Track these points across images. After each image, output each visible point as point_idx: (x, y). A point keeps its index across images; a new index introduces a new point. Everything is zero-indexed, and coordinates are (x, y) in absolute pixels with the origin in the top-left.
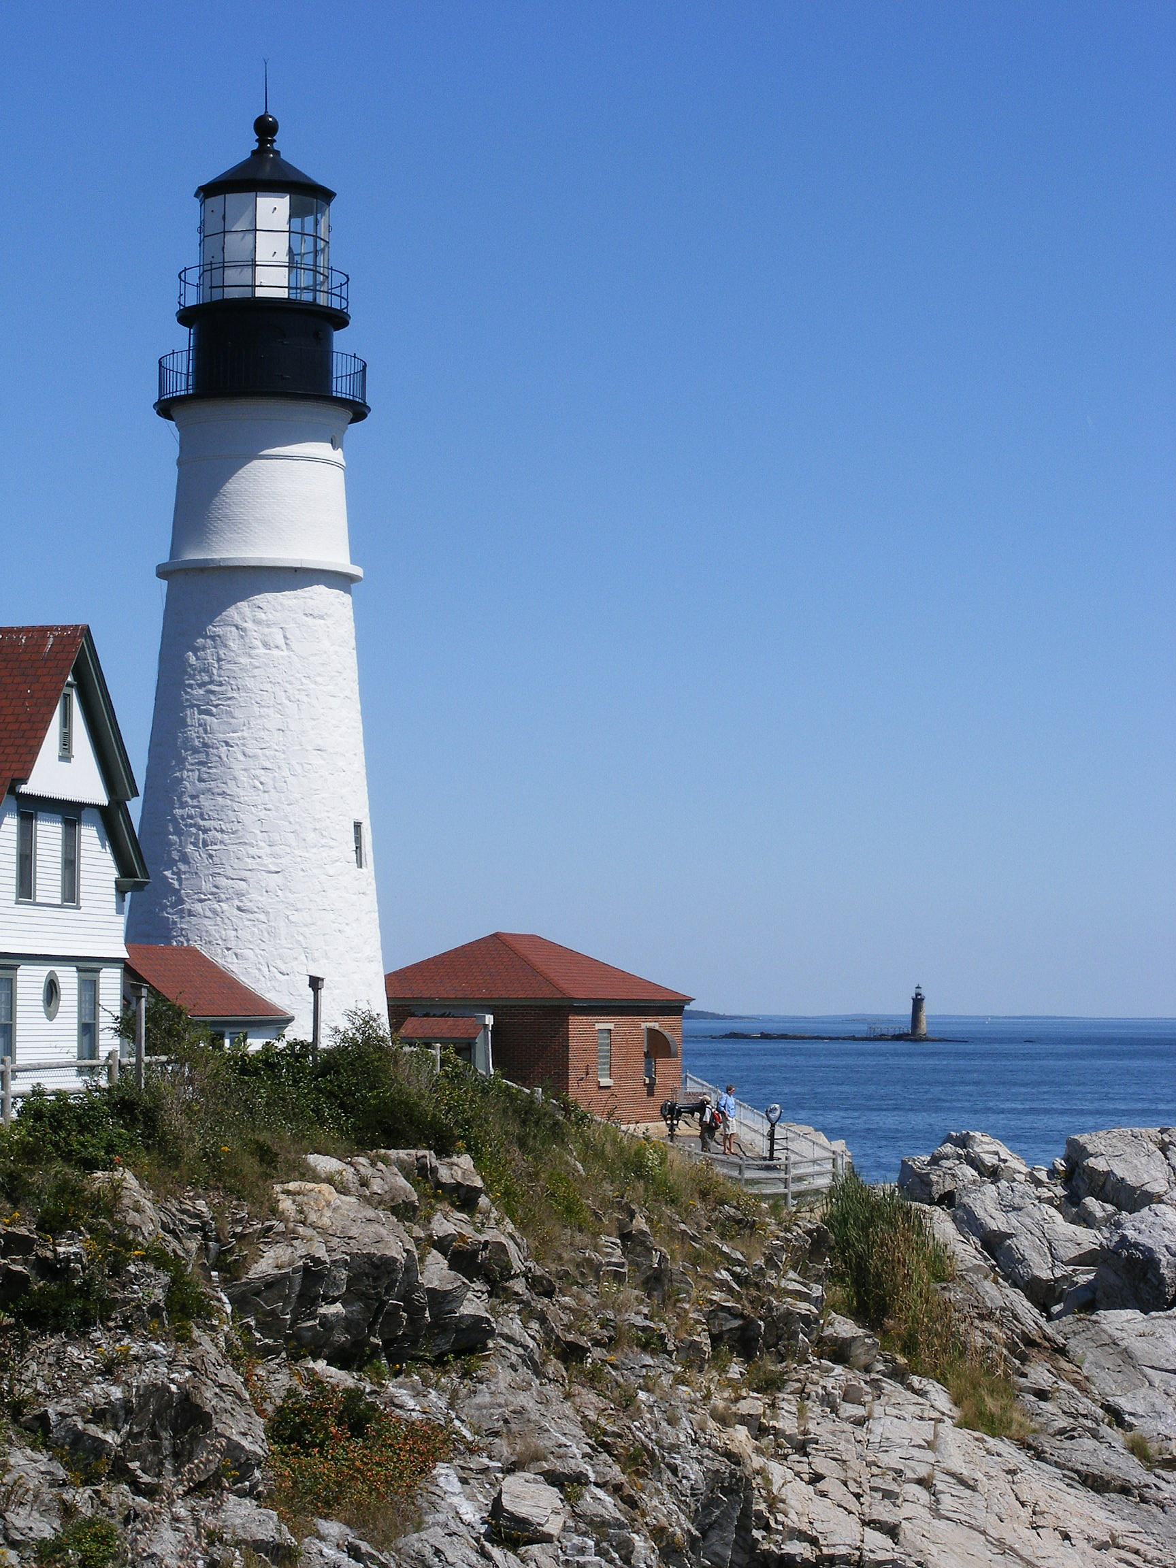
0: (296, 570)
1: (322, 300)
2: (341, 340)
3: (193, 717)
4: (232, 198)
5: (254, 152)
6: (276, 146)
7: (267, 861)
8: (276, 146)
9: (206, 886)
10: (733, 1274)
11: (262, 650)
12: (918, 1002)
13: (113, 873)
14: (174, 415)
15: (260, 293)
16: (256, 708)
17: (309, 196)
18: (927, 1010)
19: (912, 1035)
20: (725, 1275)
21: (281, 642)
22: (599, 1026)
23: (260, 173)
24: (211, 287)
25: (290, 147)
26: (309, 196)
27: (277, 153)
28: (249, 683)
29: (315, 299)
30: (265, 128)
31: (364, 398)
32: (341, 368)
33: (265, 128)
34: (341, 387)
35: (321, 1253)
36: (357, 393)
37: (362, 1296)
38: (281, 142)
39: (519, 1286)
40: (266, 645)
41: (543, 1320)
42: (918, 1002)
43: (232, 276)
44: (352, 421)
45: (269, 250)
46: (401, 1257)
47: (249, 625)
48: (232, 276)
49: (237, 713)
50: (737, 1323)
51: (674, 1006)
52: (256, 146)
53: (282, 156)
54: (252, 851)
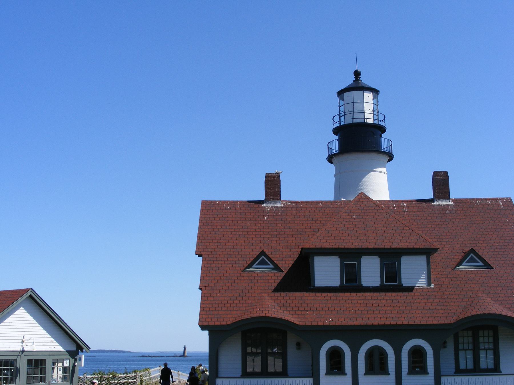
1: (382, 123)
12: (185, 349)
17: (375, 92)
18: (187, 350)
19: (183, 356)
23: (358, 86)
25: (365, 80)
26: (375, 92)
30: (357, 74)
33: (357, 74)
42: (185, 349)
43: (356, 116)
44: (389, 161)
48: (356, 116)
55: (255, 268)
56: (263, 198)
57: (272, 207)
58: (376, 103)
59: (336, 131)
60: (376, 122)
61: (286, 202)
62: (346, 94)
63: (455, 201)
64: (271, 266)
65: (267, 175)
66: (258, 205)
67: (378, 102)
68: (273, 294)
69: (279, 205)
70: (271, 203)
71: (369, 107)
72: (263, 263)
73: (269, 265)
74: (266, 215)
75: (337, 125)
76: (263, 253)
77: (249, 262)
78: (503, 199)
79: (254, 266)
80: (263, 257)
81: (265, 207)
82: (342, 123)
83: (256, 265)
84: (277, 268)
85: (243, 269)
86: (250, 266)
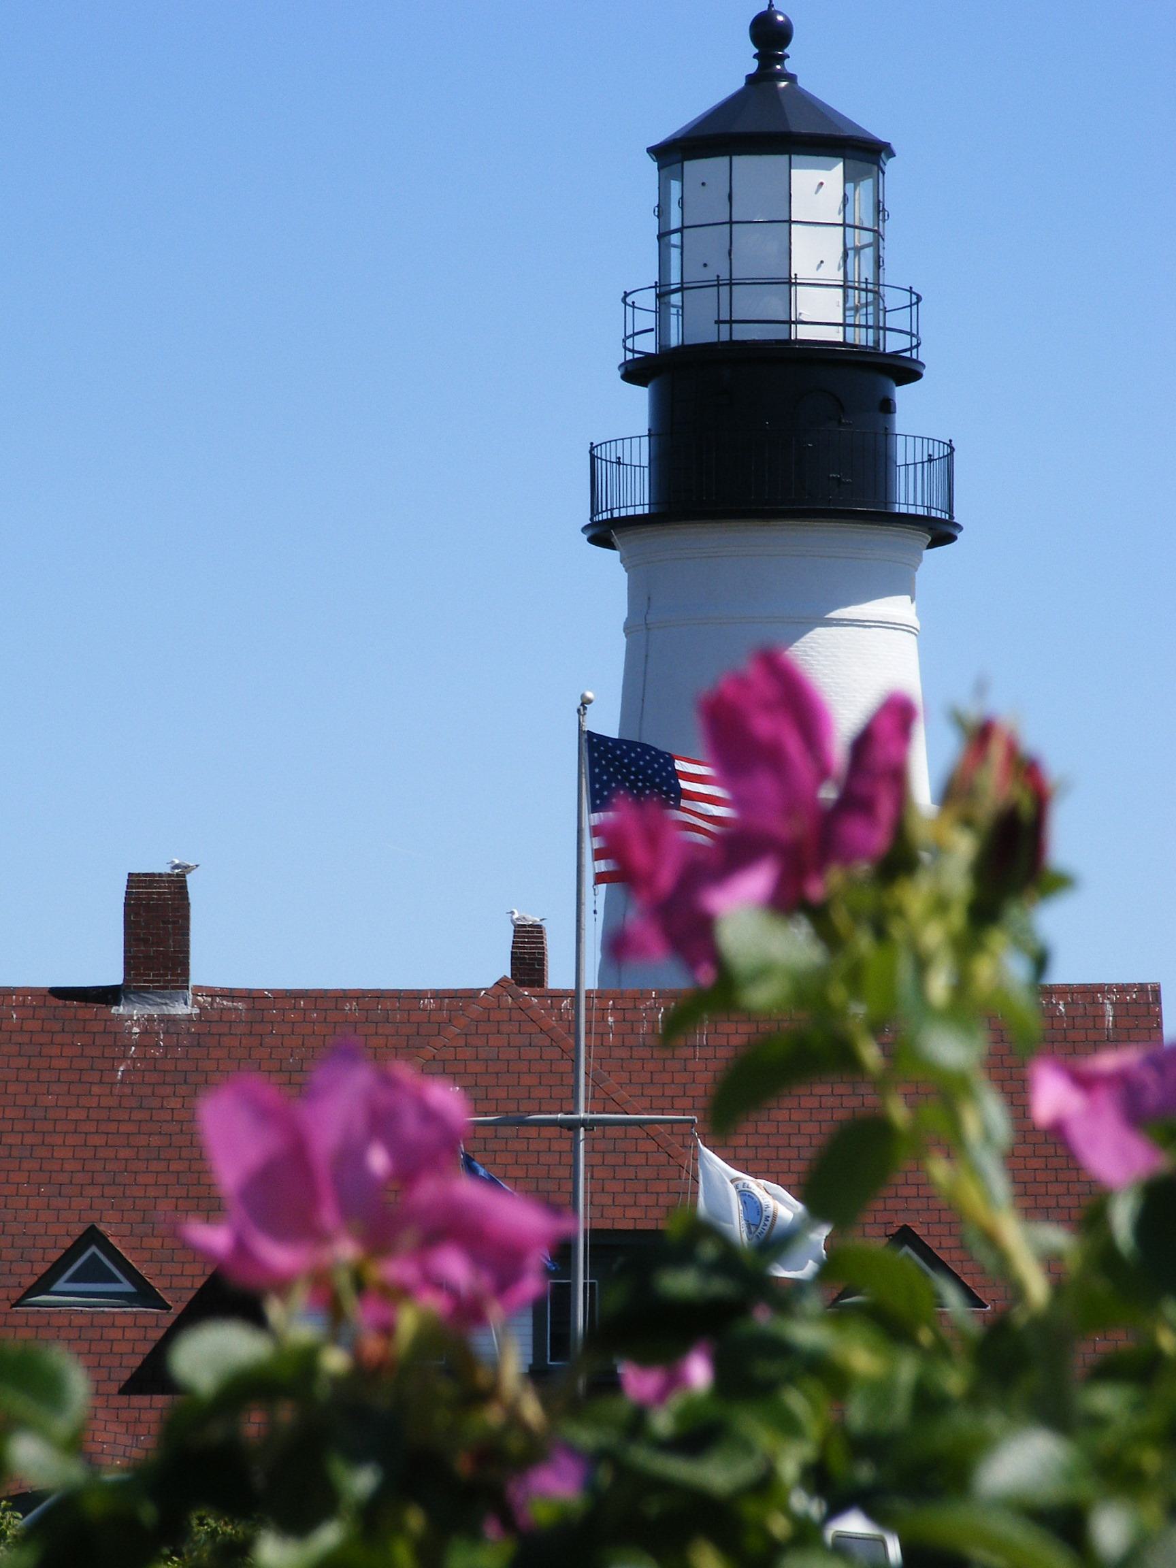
1: (894, 343)
4: (745, 164)
5: (751, 79)
6: (790, 66)
8: (790, 66)
14: (615, 539)
15: (803, 333)
24: (718, 322)
27: (791, 78)
29: (877, 342)
30: (770, 35)
31: (951, 517)
33: (770, 35)
34: (909, 494)
36: (939, 500)
43: (748, 303)
45: (814, 261)
52: (753, 66)
53: (802, 83)
55: (65, 1295)
56: (113, 975)
57: (150, 1019)
58: (862, 212)
59: (635, 371)
60: (861, 338)
61: (213, 993)
62: (693, 167)
64: (126, 1286)
65: (135, 881)
66: (95, 1008)
67: (879, 209)
68: (124, 1400)
69: (181, 1009)
70: (145, 1001)
71: (815, 254)
72: (93, 1272)
73: (118, 1281)
74: (125, 1058)
75: (647, 345)
76: (92, 1236)
77: (42, 1268)
78: (1123, 989)
79: (60, 1285)
80: (94, 1249)
81: (121, 1019)
82: (674, 341)
83: (70, 1280)
84: (145, 1295)
85: (16, 1294)
86: (43, 1284)
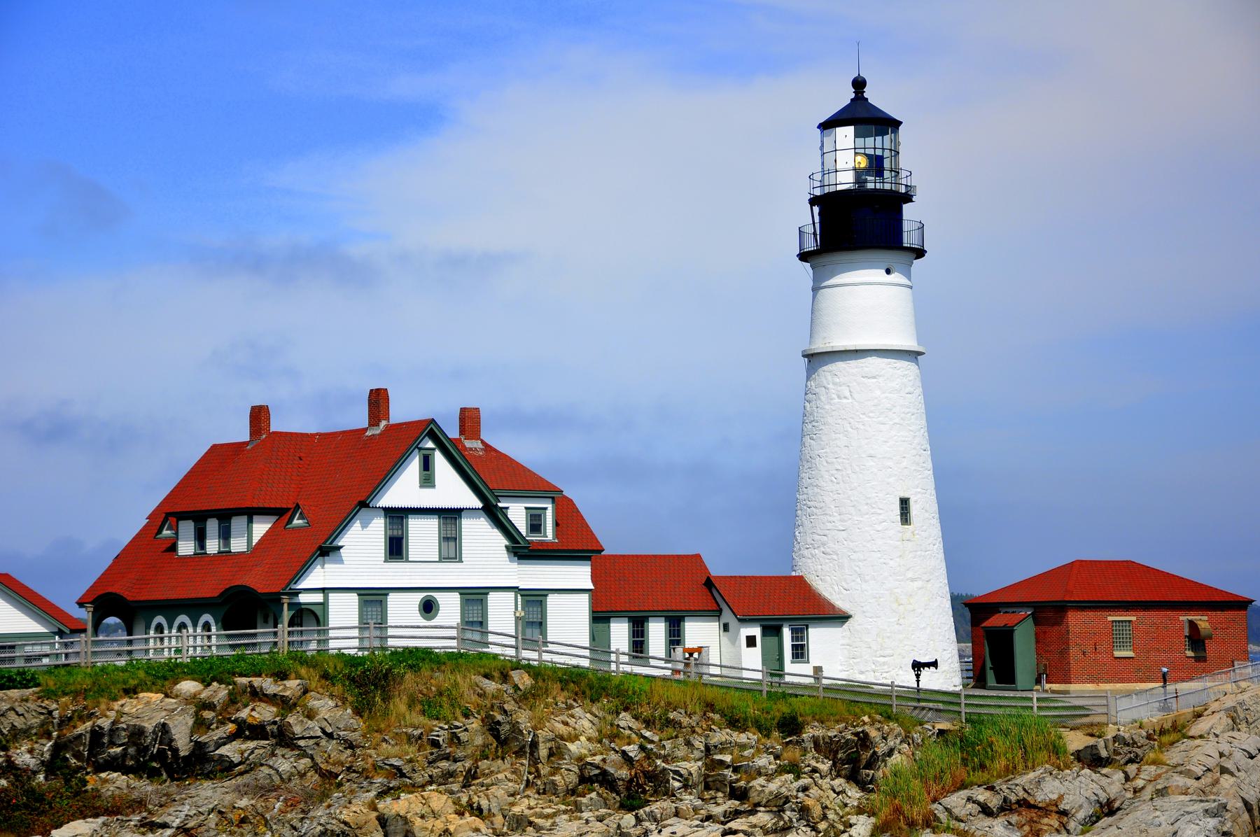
0: (857, 351)
2: (906, 207)
3: (807, 440)
7: (838, 524)
9: (809, 540)
10: (642, 748)
11: (837, 400)
13: (501, 541)
15: (840, 188)
16: (834, 436)
20: (632, 750)
21: (848, 394)
22: (1110, 618)
28: (830, 420)
30: (859, 84)
32: (906, 226)
33: (859, 84)
35: (105, 723)
37: (135, 744)
38: (868, 93)
39: (302, 743)
40: (839, 397)
41: (312, 758)
46: (149, 726)
47: (830, 386)
49: (824, 438)
50: (597, 772)
51: (1241, 604)
52: (853, 96)
54: (831, 519)
63: (392, 428)
